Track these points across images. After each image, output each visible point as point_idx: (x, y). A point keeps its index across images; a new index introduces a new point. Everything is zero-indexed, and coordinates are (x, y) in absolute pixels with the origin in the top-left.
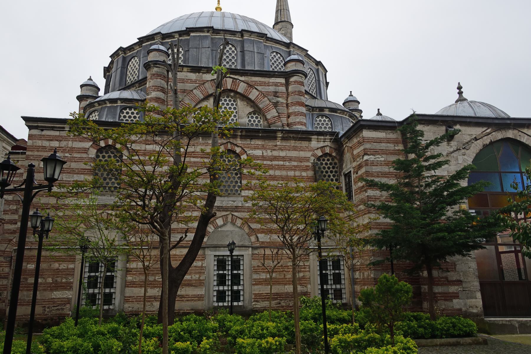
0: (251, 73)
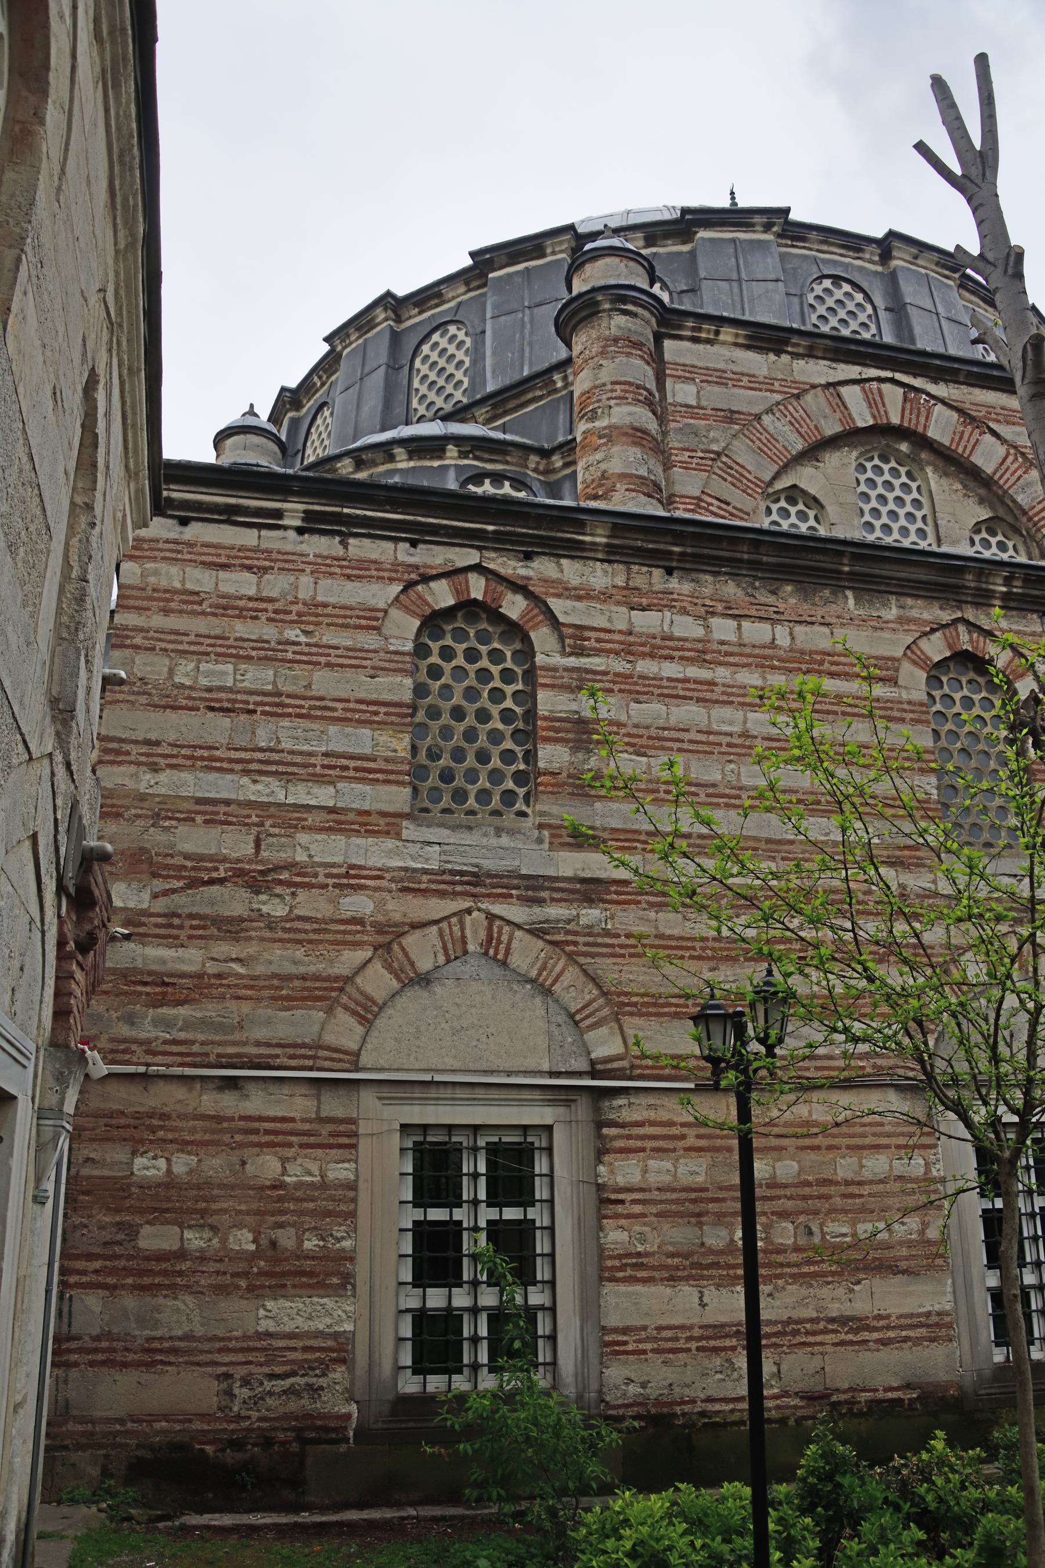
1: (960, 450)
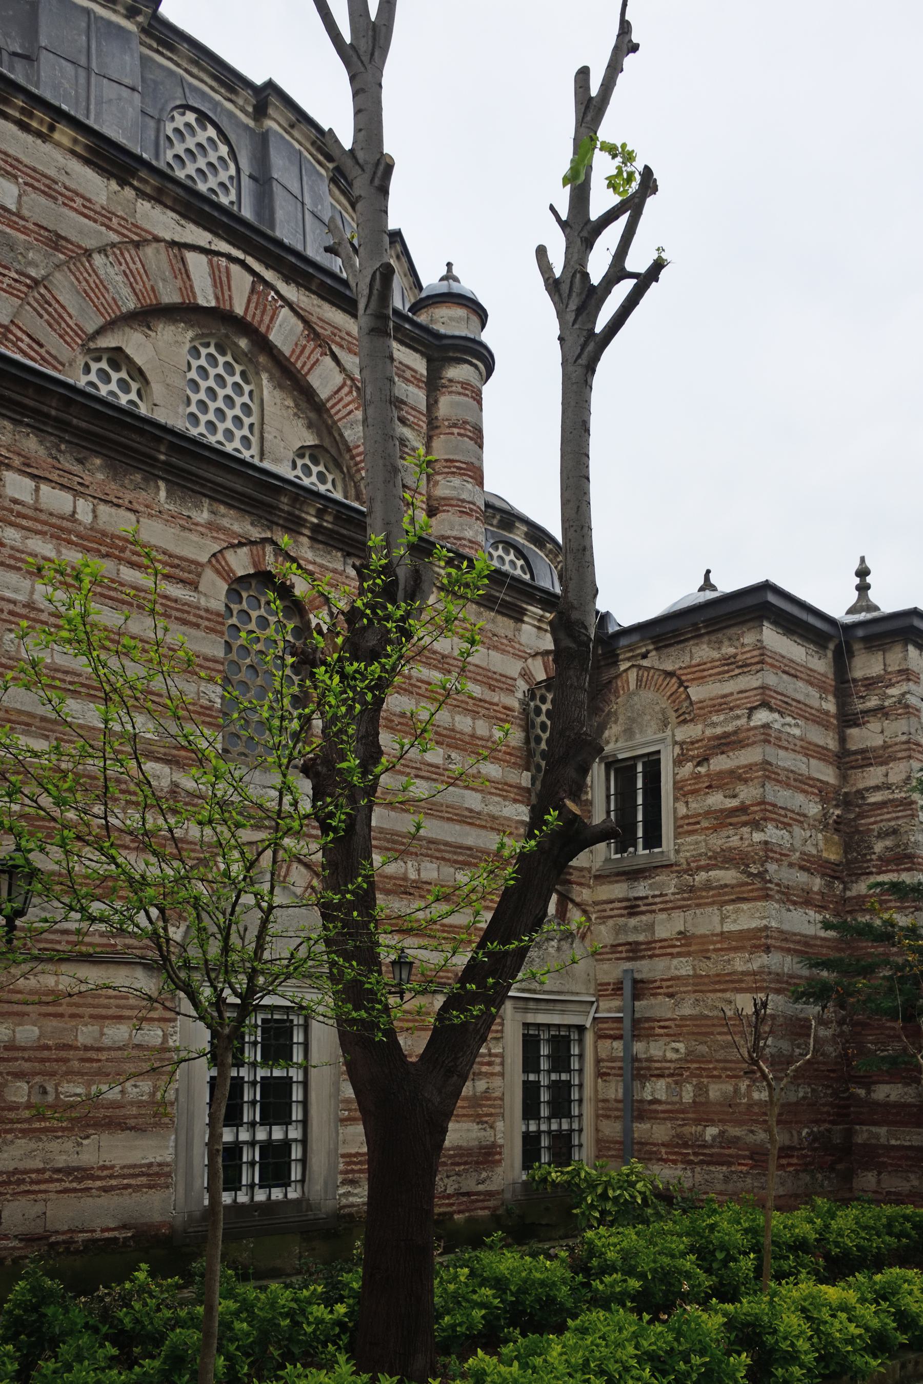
0: (323, 283)
1: (299, 365)
